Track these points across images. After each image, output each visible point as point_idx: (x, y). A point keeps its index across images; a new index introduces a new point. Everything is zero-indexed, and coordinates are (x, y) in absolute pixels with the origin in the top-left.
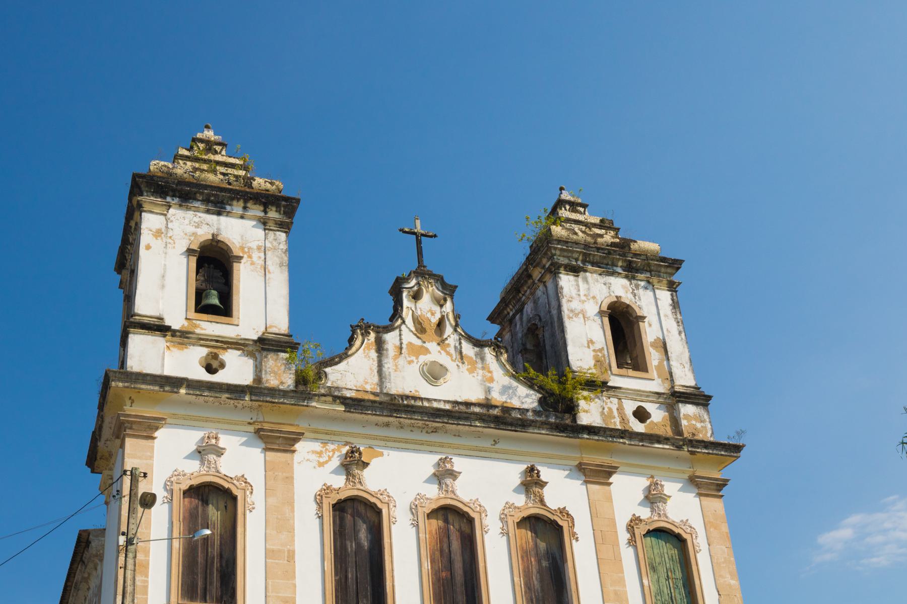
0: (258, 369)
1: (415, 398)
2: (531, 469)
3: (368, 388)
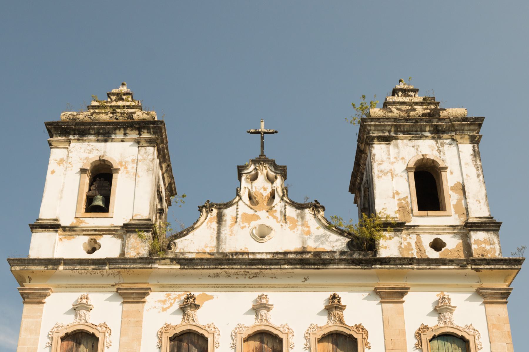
0: (123, 246)
1: (242, 254)
3: (208, 250)
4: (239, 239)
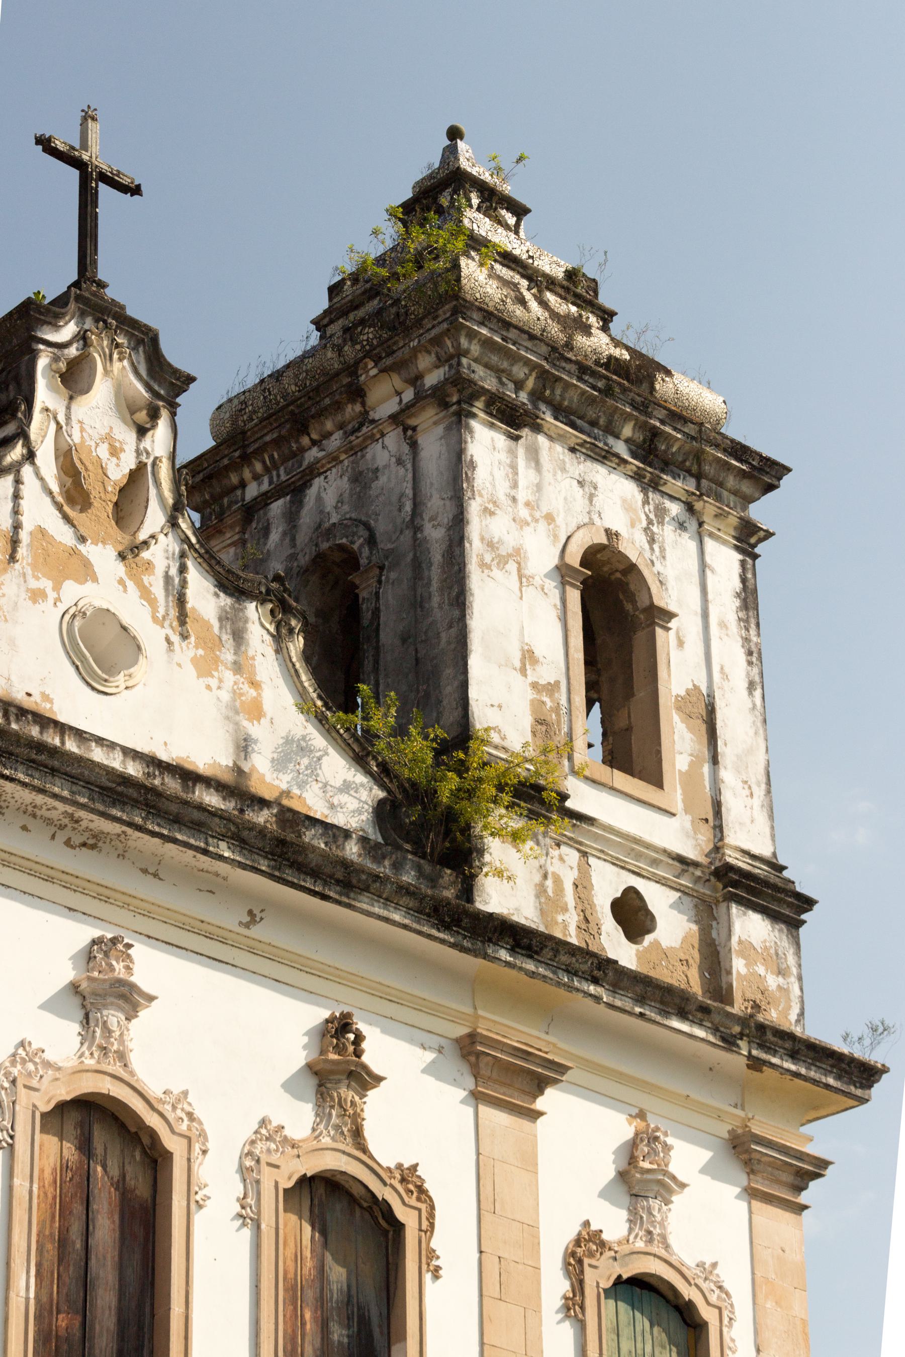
2: (340, 1029)
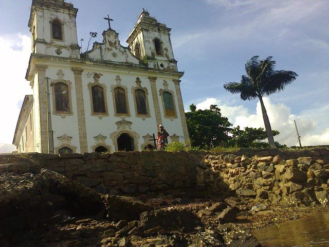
2: (138, 78)
4: (108, 57)
